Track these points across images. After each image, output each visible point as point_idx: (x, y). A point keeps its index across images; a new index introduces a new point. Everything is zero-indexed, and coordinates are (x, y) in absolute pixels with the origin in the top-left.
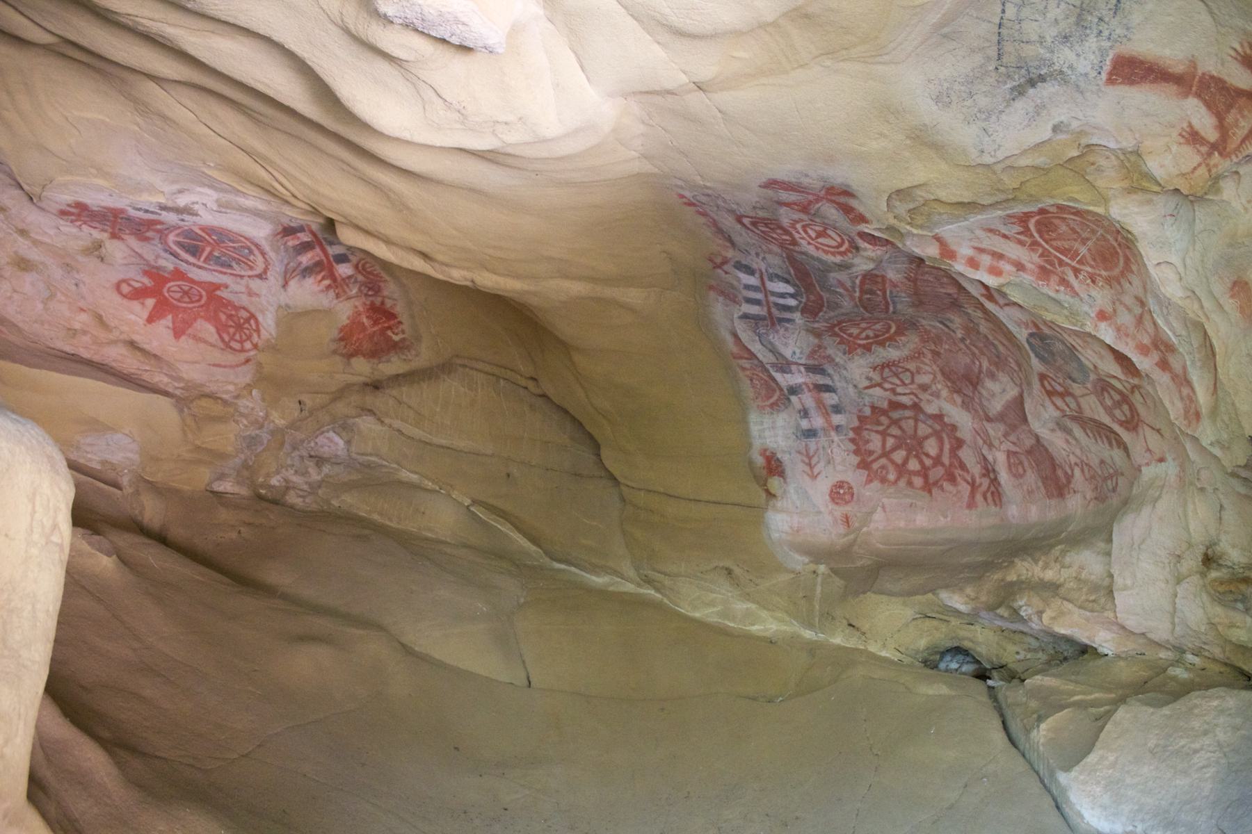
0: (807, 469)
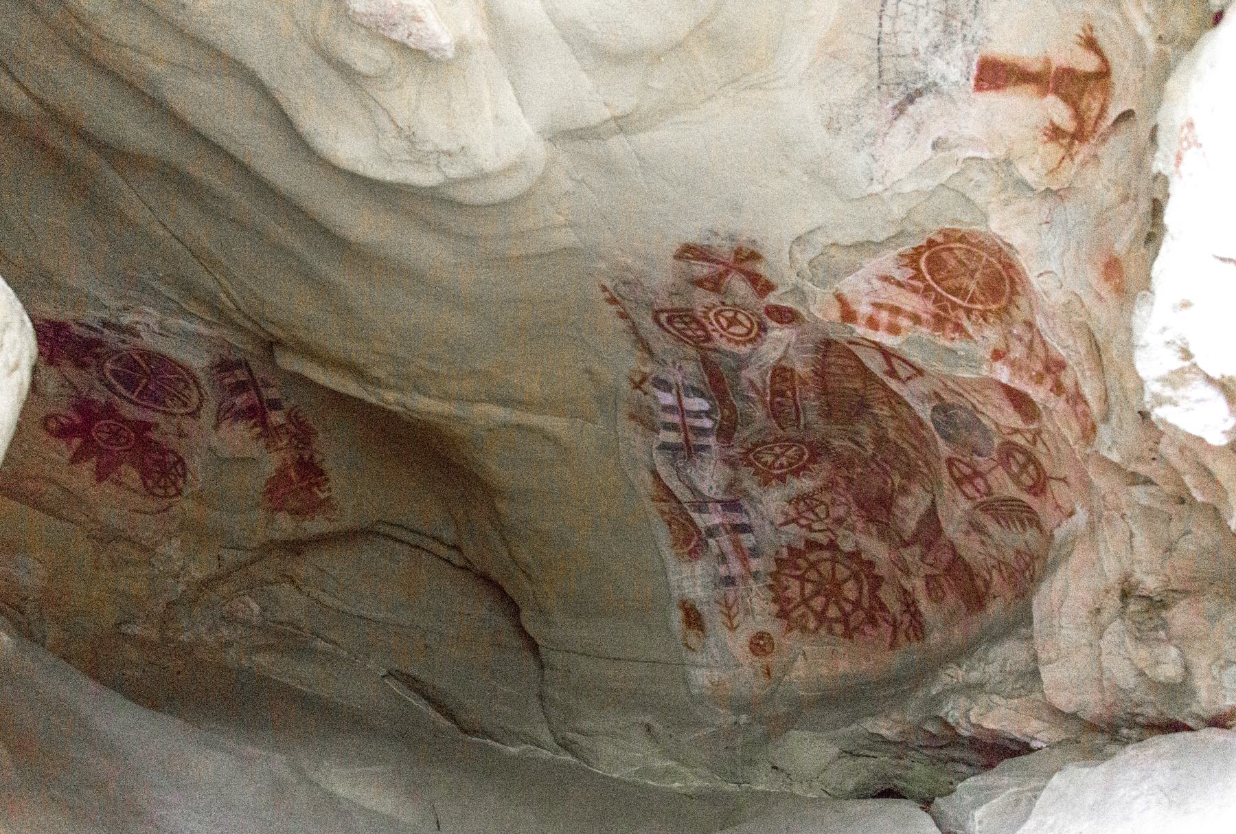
0: (726, 619)
